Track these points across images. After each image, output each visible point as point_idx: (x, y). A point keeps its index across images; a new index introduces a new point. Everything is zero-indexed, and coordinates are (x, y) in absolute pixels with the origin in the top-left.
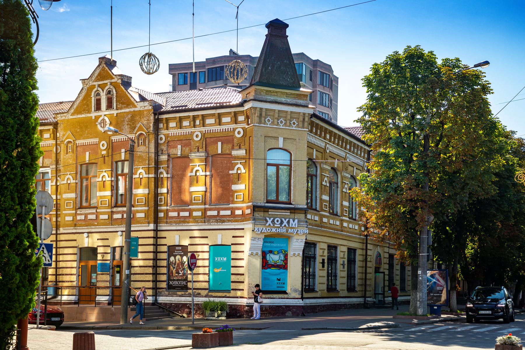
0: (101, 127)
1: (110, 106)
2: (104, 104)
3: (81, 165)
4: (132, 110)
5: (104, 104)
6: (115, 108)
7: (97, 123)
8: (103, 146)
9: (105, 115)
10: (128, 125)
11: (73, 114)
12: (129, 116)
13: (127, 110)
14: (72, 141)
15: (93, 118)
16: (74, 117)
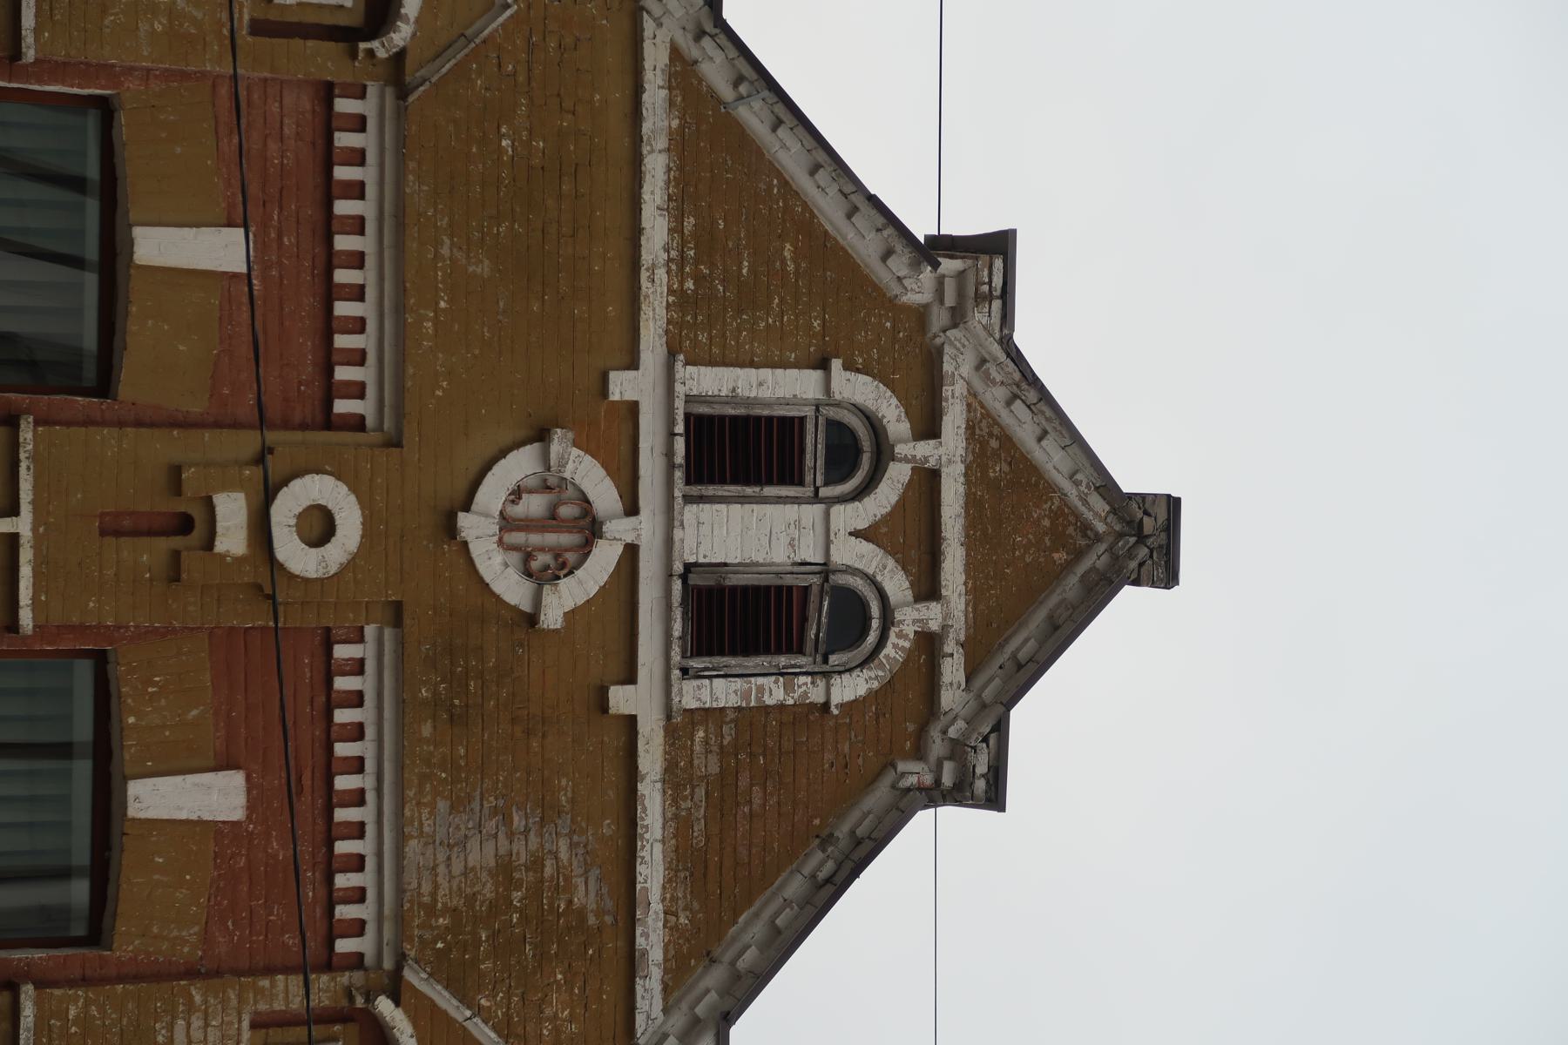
0: (517, 494)
1: (736, 617)
2: (752, 534)
3: (105, 109)
4: (652, 939)
5: (752, 534)
6: (692, 695)
7: (559, 443)
8: (318, 528)
9: (631, 551)
10: (504, 870)
11: (682, 71)
12: (586, 894)
13: (652, 872)
14: (401, 35)
15: (622, 386)
16: (655, 95)
